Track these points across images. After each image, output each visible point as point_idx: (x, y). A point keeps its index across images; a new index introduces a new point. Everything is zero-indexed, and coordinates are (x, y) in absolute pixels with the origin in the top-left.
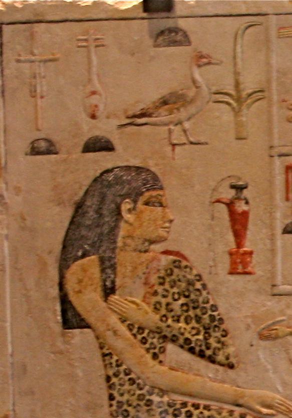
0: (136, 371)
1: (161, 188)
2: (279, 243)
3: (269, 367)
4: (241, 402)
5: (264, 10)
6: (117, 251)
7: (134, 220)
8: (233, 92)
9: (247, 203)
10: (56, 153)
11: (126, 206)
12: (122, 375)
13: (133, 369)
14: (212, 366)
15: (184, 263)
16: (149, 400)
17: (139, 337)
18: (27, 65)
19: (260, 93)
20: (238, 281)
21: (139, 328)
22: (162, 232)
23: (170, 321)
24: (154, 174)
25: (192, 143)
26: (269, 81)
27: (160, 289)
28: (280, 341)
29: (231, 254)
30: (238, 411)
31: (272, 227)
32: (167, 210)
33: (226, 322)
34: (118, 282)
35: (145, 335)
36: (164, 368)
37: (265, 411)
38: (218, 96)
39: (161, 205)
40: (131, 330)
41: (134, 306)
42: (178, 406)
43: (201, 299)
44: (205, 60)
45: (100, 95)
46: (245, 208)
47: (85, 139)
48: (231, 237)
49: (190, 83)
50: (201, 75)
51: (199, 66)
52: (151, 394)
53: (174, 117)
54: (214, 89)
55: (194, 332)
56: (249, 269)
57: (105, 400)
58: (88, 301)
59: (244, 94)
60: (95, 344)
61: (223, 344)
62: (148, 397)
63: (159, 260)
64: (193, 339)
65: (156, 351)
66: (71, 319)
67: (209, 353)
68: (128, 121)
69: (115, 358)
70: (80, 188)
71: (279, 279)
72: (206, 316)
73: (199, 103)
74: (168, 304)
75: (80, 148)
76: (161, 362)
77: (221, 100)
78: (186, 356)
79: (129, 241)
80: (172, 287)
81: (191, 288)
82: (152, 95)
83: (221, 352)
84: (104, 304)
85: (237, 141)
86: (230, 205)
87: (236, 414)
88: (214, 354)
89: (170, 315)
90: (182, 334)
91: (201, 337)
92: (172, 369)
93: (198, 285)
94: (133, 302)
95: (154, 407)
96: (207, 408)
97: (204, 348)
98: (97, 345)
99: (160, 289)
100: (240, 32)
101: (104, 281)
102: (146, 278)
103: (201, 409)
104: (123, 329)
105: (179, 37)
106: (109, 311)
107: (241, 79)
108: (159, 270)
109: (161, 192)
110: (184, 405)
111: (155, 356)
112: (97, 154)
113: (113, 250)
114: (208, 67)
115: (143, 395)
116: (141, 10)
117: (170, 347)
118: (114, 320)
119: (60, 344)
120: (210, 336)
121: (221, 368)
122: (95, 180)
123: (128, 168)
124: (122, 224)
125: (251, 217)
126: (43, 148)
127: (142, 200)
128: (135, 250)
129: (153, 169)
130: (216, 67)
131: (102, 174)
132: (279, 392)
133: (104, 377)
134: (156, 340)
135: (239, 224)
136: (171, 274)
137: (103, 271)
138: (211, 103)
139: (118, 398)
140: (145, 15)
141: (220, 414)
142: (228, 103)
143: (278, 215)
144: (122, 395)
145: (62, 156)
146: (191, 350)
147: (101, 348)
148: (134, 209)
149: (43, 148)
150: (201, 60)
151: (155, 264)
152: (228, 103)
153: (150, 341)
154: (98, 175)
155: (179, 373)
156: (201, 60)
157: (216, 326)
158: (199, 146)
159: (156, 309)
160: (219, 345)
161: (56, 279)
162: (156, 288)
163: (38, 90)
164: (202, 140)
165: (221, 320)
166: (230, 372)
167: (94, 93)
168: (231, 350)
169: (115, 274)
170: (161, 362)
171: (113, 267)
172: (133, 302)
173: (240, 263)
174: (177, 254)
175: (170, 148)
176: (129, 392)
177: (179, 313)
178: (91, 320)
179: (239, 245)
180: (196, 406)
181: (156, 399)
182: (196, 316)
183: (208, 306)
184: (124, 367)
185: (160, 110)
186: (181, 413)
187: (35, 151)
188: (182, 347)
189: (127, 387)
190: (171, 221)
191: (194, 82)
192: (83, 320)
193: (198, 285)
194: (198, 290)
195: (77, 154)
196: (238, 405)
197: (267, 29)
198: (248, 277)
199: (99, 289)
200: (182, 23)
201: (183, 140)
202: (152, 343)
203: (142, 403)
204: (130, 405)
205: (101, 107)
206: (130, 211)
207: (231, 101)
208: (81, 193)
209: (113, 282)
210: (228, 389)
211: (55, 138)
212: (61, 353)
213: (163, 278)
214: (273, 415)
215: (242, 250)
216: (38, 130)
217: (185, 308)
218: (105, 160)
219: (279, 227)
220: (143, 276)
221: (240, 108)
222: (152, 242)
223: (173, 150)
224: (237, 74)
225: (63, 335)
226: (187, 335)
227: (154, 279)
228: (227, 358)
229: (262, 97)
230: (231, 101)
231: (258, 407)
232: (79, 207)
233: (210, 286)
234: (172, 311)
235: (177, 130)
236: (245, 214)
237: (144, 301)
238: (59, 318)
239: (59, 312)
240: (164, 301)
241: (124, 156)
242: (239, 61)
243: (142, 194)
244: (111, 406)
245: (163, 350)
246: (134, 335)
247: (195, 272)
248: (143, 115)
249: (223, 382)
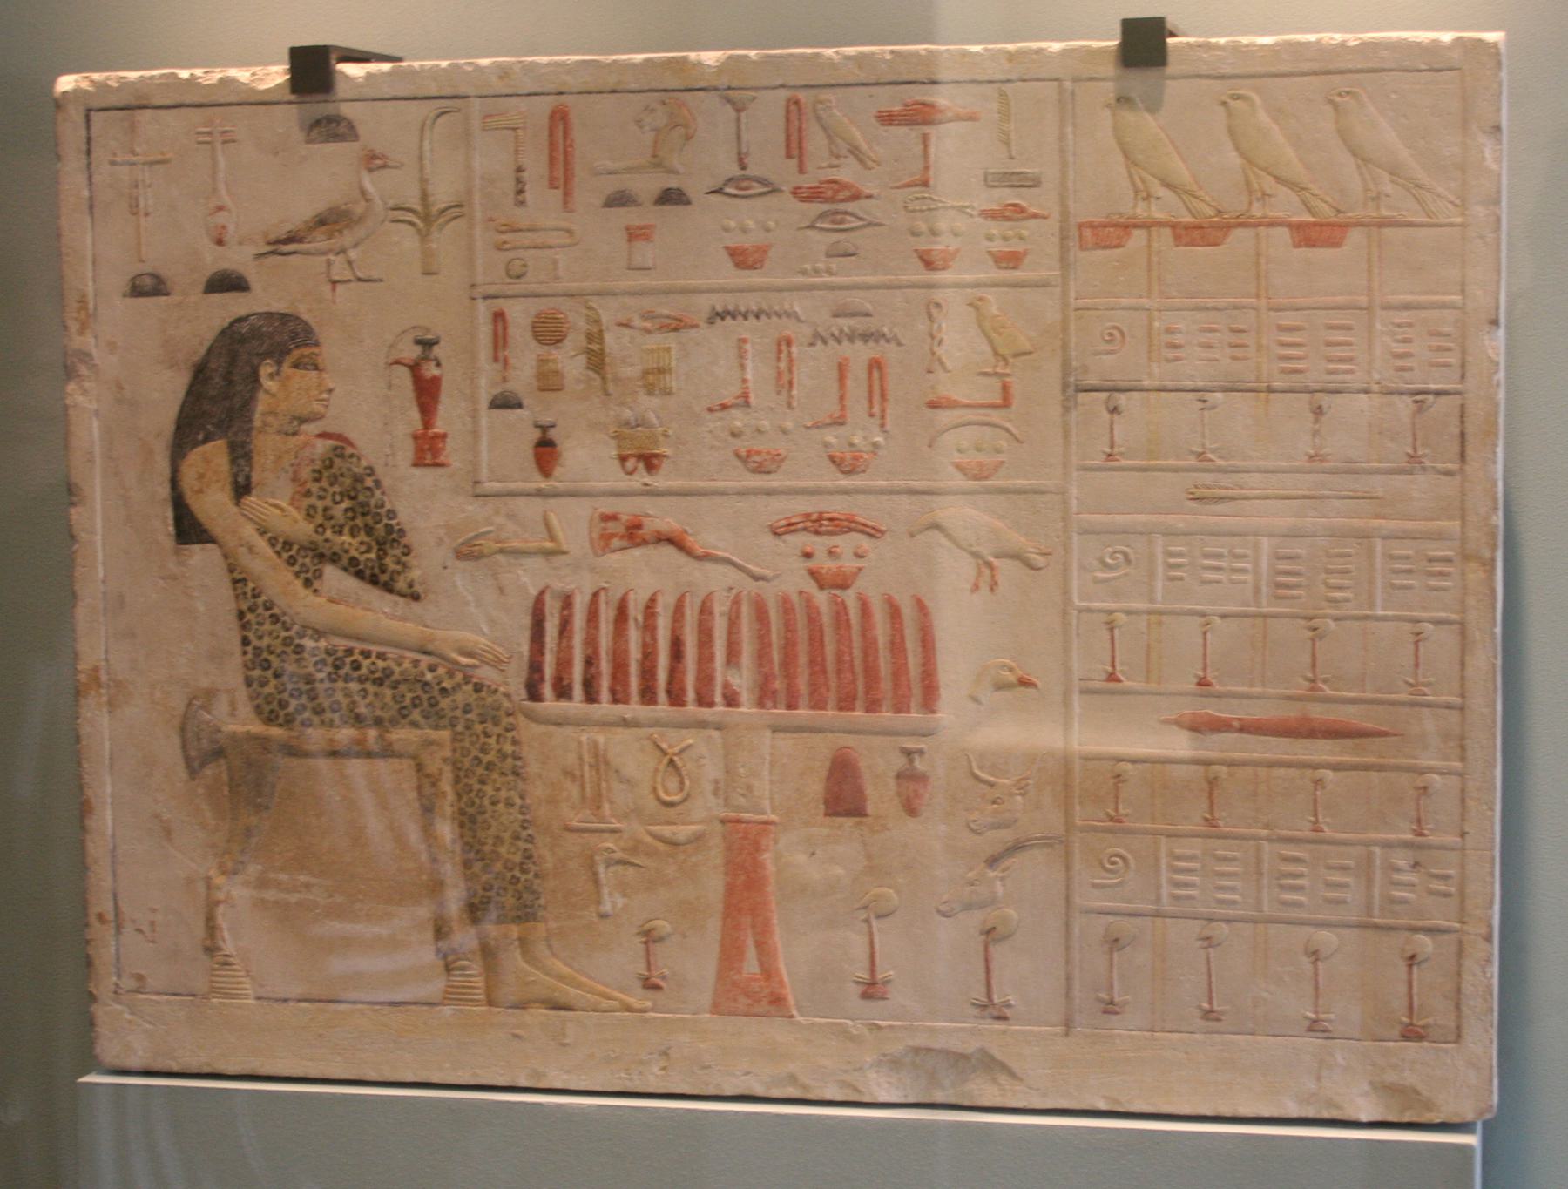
0: (281, 602)
1: (317, 344)
2: (484, 422)
3: (470, 598)
4: (430, 647)
5: (463, 90)
6: (254, 433)
7: (277, 390)
8: (418, 207)
9: (438, 365)
10: (167, 294)
11: (266, 369)
12: (260, 610)
13: (276, 601)
14: (388, 596)
15: (349, 450)
16: (299, 646)
17: (285, 555)
18: (125, 169)
19: (457, 209)
20: (425, 477)
21: (285, 543)
22: (317, 407)
23: (329, 533)
24: (306, 323)
25: (360, 280)
26: (469, 192)
27: (314, 488)
28: (485, 560)
29: (415, 437)
30: (425, 660)
31: (473, 400)
32: (325, 375)
33: (409, 534)
34: (255, 477)
35: (293, 552)
36: (321, 600)
37: (464, 660)
38: (396, 213)
39: (316, 368)
40: (273, 546)
41: (278, 512)
42: (340, 654)
43: (373, 502)
44: (378, 162)
45: (229, 211)
46: (435, 372)
47: (208, 274)
48: (415, 414)
51: (370, 170)
52: (302, 637)
53: (336, 242)
54: (391, 203)
55: (363, 548)
56: (442, 459)
57: (237, 648)
58: (213, 504)
60: (221, 565)
61: (404, 565)
62: (297, 641)
63: (314, 446)
64: (362, 558)
65: (309, 575)
66: (189, 529)
67: (384, 578)
68: (269, 248)
69: (251, 585)
70: (201, 344)
71: (484, 473)
72: (380, 526)
74: (326, 509)
75: (201, 287)
76: (315, 591)
78: (350, 583)
79: (270, 419)
80: (332, 485)
81: (359, 486)
82: (302, 210)
83: (401, 578)
84: (235, 509)
86: (415, 368)
87: (423, 666)
88: (392, 579)
89: (328, 524)
90: (346, 551)
91: (372, 556)
92: (332, 601)
93: (369, 482)
94: (276, 506)
95: (306, 655)
96: (381, 656)
97: (377, 571)
98: (225, 567)
99: (314, 488)
101: (235, 476)
102: (295, 473)
103: (373, 659)
104: (262, 544)
105: (342, 129)
106: (242, 520)
107: (430, 188)
108: (313, 461)
109: (316, 350)
110: (349, 652)
111: (308, 583)
112: (226, 295)
113: (248, 432)
114: (384, 172)
115: (290, 638)
116: (288, 90)
117: (330, 571)
118: (249, 531)
119: (172, 565)
120: (386, 554)
121: (401, 600)
122: (223, 332)
123: (269, 315)
124: (261, 396)
125: (445, 385)
126: (148, 287)
127: (288, 361)
128: (279, 432)
129: (305, 317)
130: (394, 171)
131: (232, 324)
132: (484, 634)
133: (235, 613)
134: (308, 559)
135: (427, 393)
136: (331, 466)
137: (233, 461)
139: (255, 642)
140: (293, 98)
141: (400, 665)
143: (483, 382)
144: (260, 638)
145: (175, 298)
146: (359, 575)
147: (231, 571)
148: (278, 373)
149: (148, 287)
150: (373, 161)
151: (307, 452)
153: (300, 561)
154: (226, 324)
155: (342, 608)
156: (373, 161)
157: (394, 540)
159: (309, 516)
160: (399, 568)
161: (167, 472)
162: (308, 485)
163: (142, 204)
164: (375, 275)
165: (402, 532)
166: (415, 606)
167: (220, 208)
168: (415, 574)
169: (251, 466)
170: (315, 591)
171: (248, 456)
172: (276, 506)
173: (428, 450)
174: (339, 437)
175: (329, 286)
176: (270, 634)
177: (342, 521)
178: (216, 529)
179: (427, 424)
180: (366, 654)
181: (309, 643)
182: (366, 525)
183: (383, 511)
184: (264, 598)
185: (315, 234)
186: (344, 664)
187: (137, 291)
188: (345, 570)
189: (267, 626)
190: (330, 391)
191: (363, 192)
192: (205, 531)
193: (369, 482)
194: (369, 489)
195: (196, 295)
196: (425, 653)
198: (440, 471)
199: (228, 487)
200: (347, 110)
201: (348, 275)
202: (303, 565)
203: (289, 650)
204: (272, 653)
205: (231, 228)
206: (271, 376)
207: (416, 220)
208: (203, 351)
209: (248, 478)
210: (410, 630)
211: (164, 272)
212: (174, 578)
213: (319, 472)
214: (475, 667)
215: (431, 432)
216: (142, 261)
217: (350, 514)
218: (234, 306)
219: (484, 399)
220: (291, 469)
222: (303, 420)
223: (334, 289)
224: (424, 181)
225: (177, 553)
226: (354, 553)
227: (306, 473)
228: (411, 586)
230: (416, 220)
231: (454, 656)
232: (200, 373)
233: (386, 482)
234: (331, 518)
235: (338, 261)
236: (436, 381)
237: (291, 505)
238: (171, 528)
239: (171, 521)
240: (320, 504)
241: (264, 298)
242: (427, 162)
243: (288, 352)
244: (245, 653)
245: (319, 575)
246: (278, 553)
247: (364, 463)
248: (290, 239)
249: (404, 619)
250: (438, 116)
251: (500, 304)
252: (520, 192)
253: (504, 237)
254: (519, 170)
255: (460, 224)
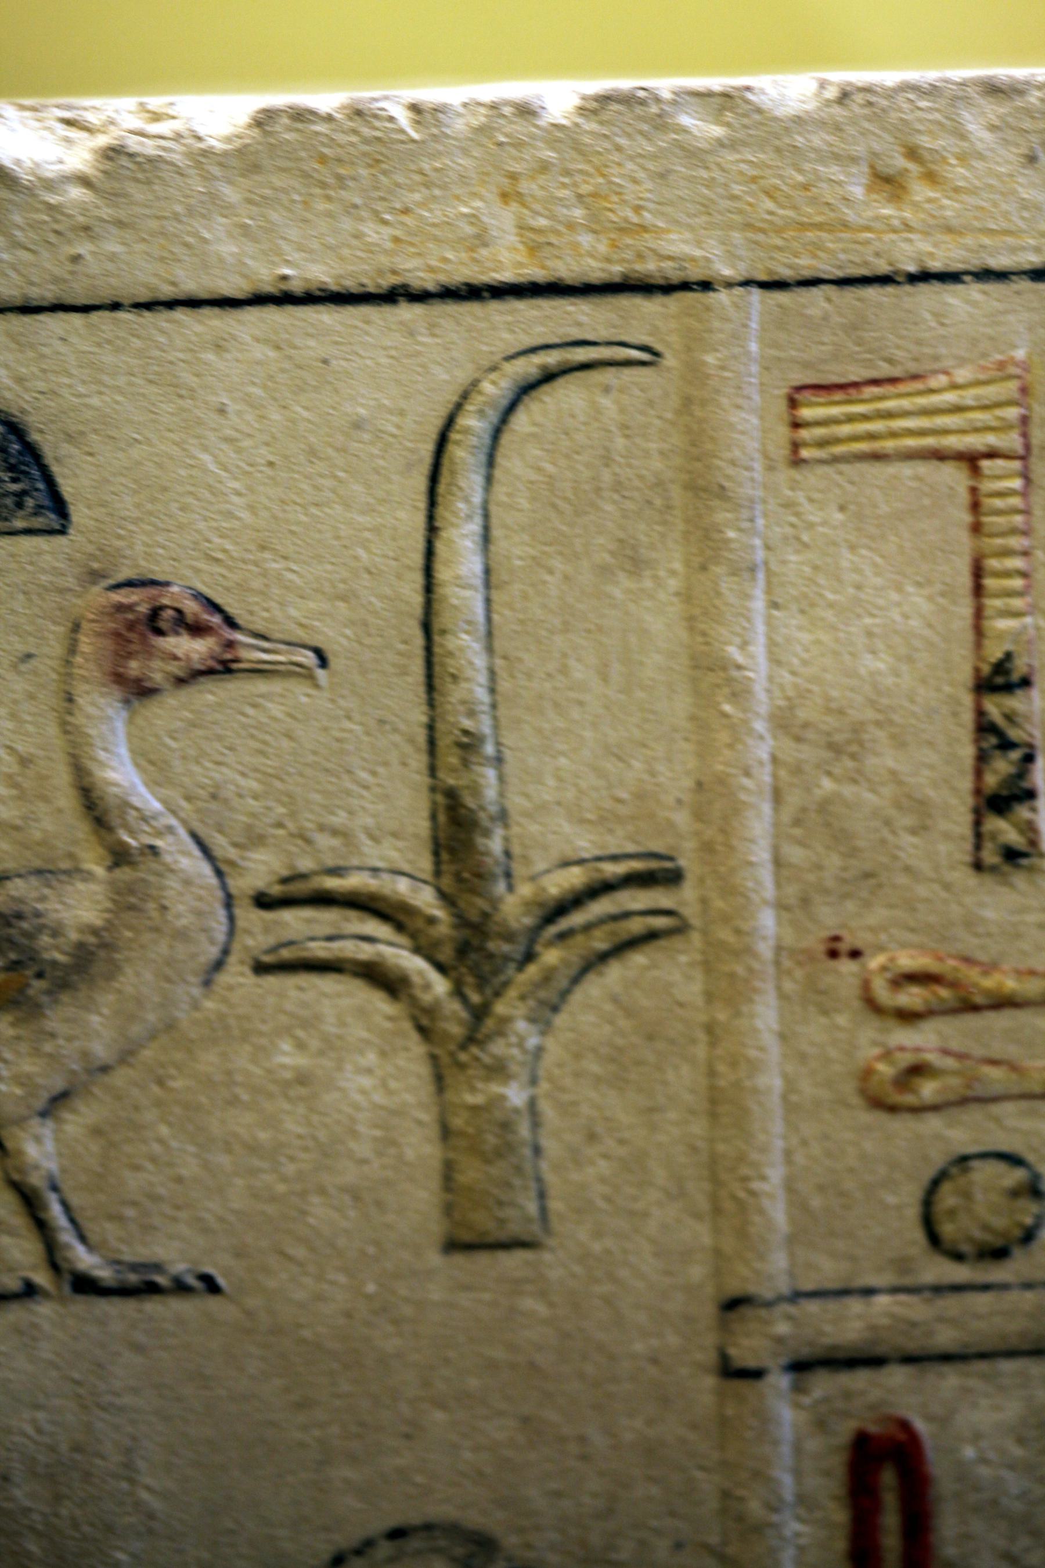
5: (679, 246)
19: (635, 900)
25: (85, 1285)
26: (713, 798)
38: (294, 921)
49: (59, 820)
50: (152, 764)
51: (140, 691)
54: (261, 869)
59: (513, 906)
73: (137, 978)
77: (319, 950)
85: (459, 1259)
100: (474, 423)
114: (210, 694)
130: (274, 701)
138: (237, 976)
142: (378, 976)
150: (155, 636)
152: (378, 976)
158: (152, 1306)
164: (176, 1256)
191: (96, 809)
197: (694, 406)
221: (479, 1013)
224: (447, 749)
229: (660, 922)
230: (414, 964)
242: (465, 647)
250: (527, 389)
251: (896, 1392)
252: (1007, 798)
253: (923, 1040)
254: (999, 679)
255: (667, 975)
